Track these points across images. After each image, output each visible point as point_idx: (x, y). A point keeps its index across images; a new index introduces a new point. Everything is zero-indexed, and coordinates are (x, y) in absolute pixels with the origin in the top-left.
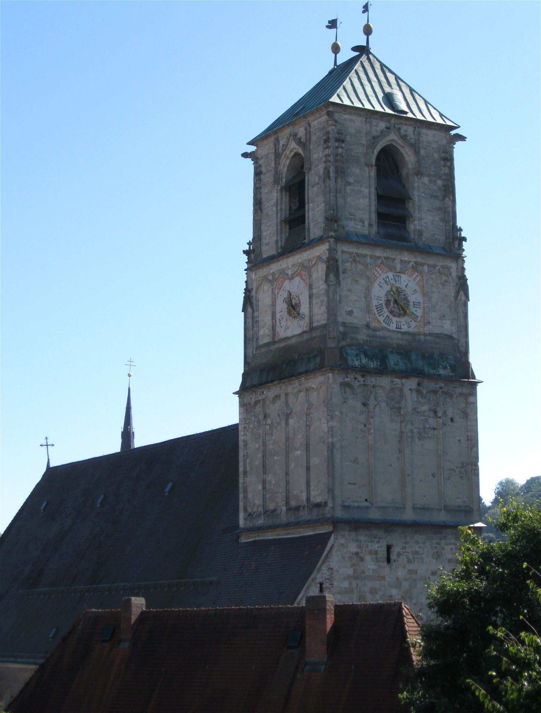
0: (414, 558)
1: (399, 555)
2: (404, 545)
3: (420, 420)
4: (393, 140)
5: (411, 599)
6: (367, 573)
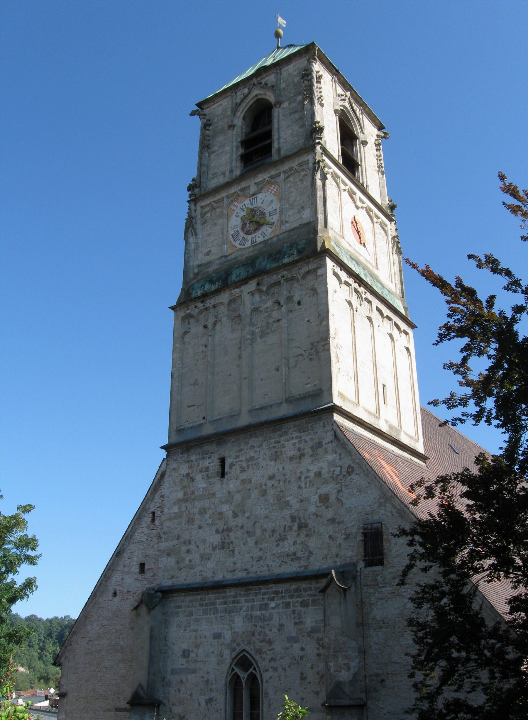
0: (248, 466)
1: (232, 465)
2: (237, 454)
3: (262, 319)
4: (256, 95)
5: (244, 513)
6: (196, 493)
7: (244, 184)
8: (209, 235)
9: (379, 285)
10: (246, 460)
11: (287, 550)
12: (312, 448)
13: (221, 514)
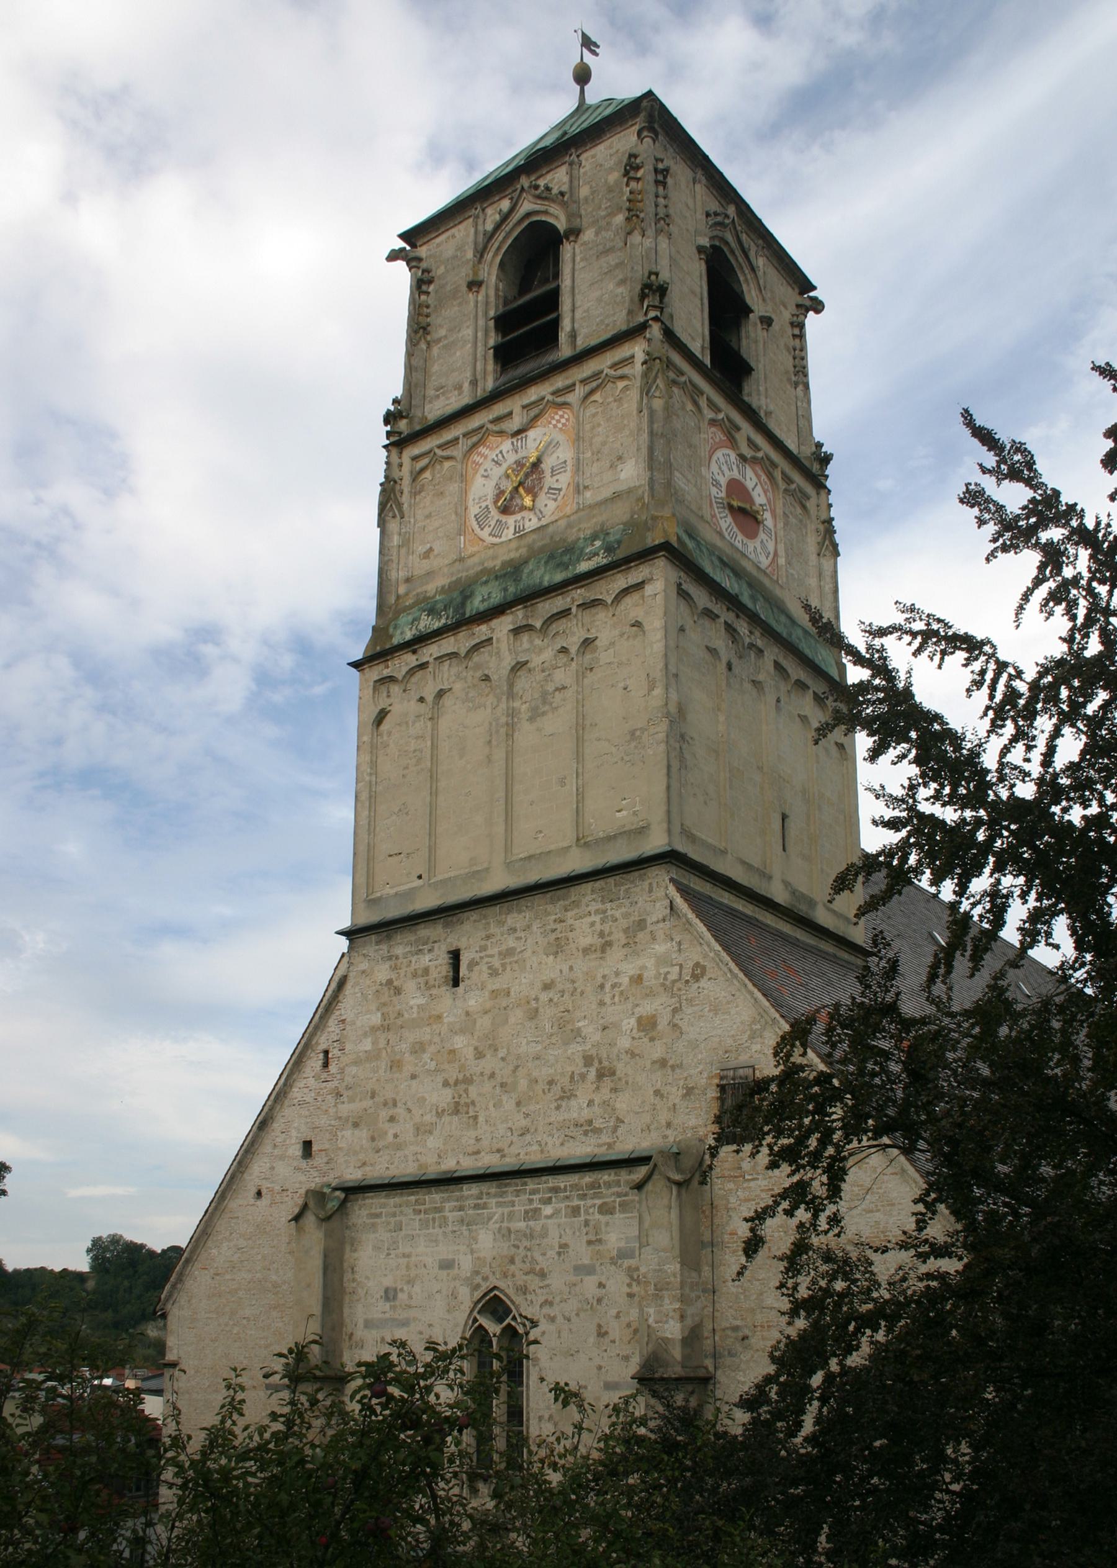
0: (503, 965)
1: (472, 964)
2: (483, 943)
3: (534, 684)
4: (528, 215)
5: (496, 1050)
7: (499, 409)
8: (429, 516)
9: (783, 619)
10: (500, 953)
11: (575, 1115)
12: (626, 931)
13: (452, 1052)
